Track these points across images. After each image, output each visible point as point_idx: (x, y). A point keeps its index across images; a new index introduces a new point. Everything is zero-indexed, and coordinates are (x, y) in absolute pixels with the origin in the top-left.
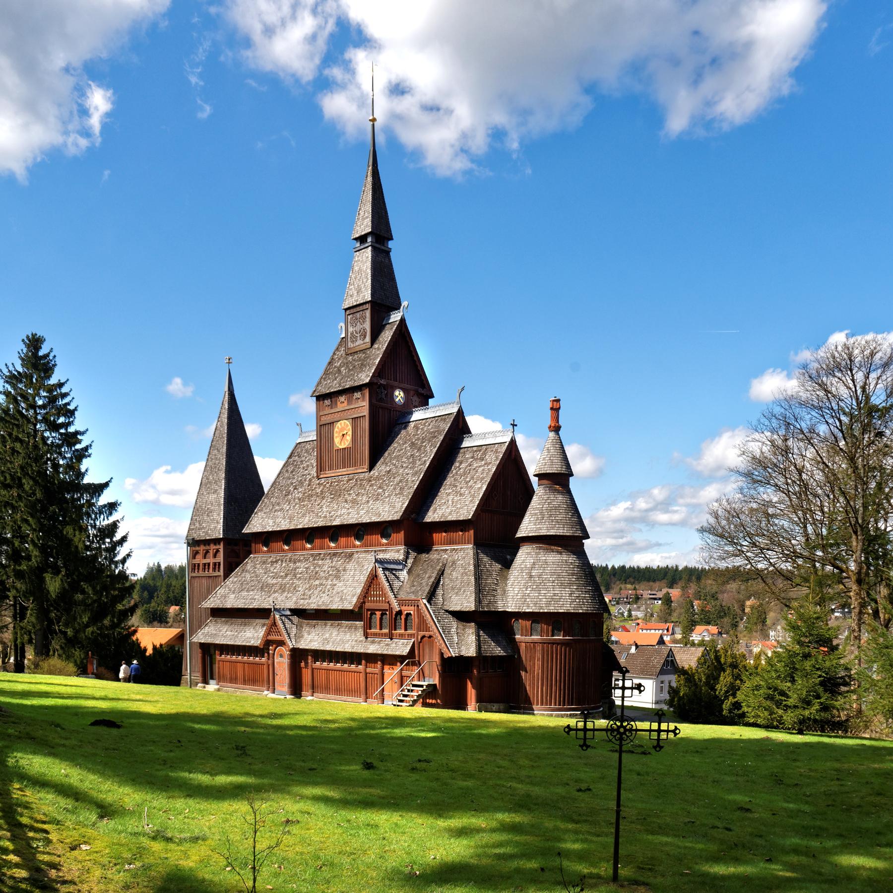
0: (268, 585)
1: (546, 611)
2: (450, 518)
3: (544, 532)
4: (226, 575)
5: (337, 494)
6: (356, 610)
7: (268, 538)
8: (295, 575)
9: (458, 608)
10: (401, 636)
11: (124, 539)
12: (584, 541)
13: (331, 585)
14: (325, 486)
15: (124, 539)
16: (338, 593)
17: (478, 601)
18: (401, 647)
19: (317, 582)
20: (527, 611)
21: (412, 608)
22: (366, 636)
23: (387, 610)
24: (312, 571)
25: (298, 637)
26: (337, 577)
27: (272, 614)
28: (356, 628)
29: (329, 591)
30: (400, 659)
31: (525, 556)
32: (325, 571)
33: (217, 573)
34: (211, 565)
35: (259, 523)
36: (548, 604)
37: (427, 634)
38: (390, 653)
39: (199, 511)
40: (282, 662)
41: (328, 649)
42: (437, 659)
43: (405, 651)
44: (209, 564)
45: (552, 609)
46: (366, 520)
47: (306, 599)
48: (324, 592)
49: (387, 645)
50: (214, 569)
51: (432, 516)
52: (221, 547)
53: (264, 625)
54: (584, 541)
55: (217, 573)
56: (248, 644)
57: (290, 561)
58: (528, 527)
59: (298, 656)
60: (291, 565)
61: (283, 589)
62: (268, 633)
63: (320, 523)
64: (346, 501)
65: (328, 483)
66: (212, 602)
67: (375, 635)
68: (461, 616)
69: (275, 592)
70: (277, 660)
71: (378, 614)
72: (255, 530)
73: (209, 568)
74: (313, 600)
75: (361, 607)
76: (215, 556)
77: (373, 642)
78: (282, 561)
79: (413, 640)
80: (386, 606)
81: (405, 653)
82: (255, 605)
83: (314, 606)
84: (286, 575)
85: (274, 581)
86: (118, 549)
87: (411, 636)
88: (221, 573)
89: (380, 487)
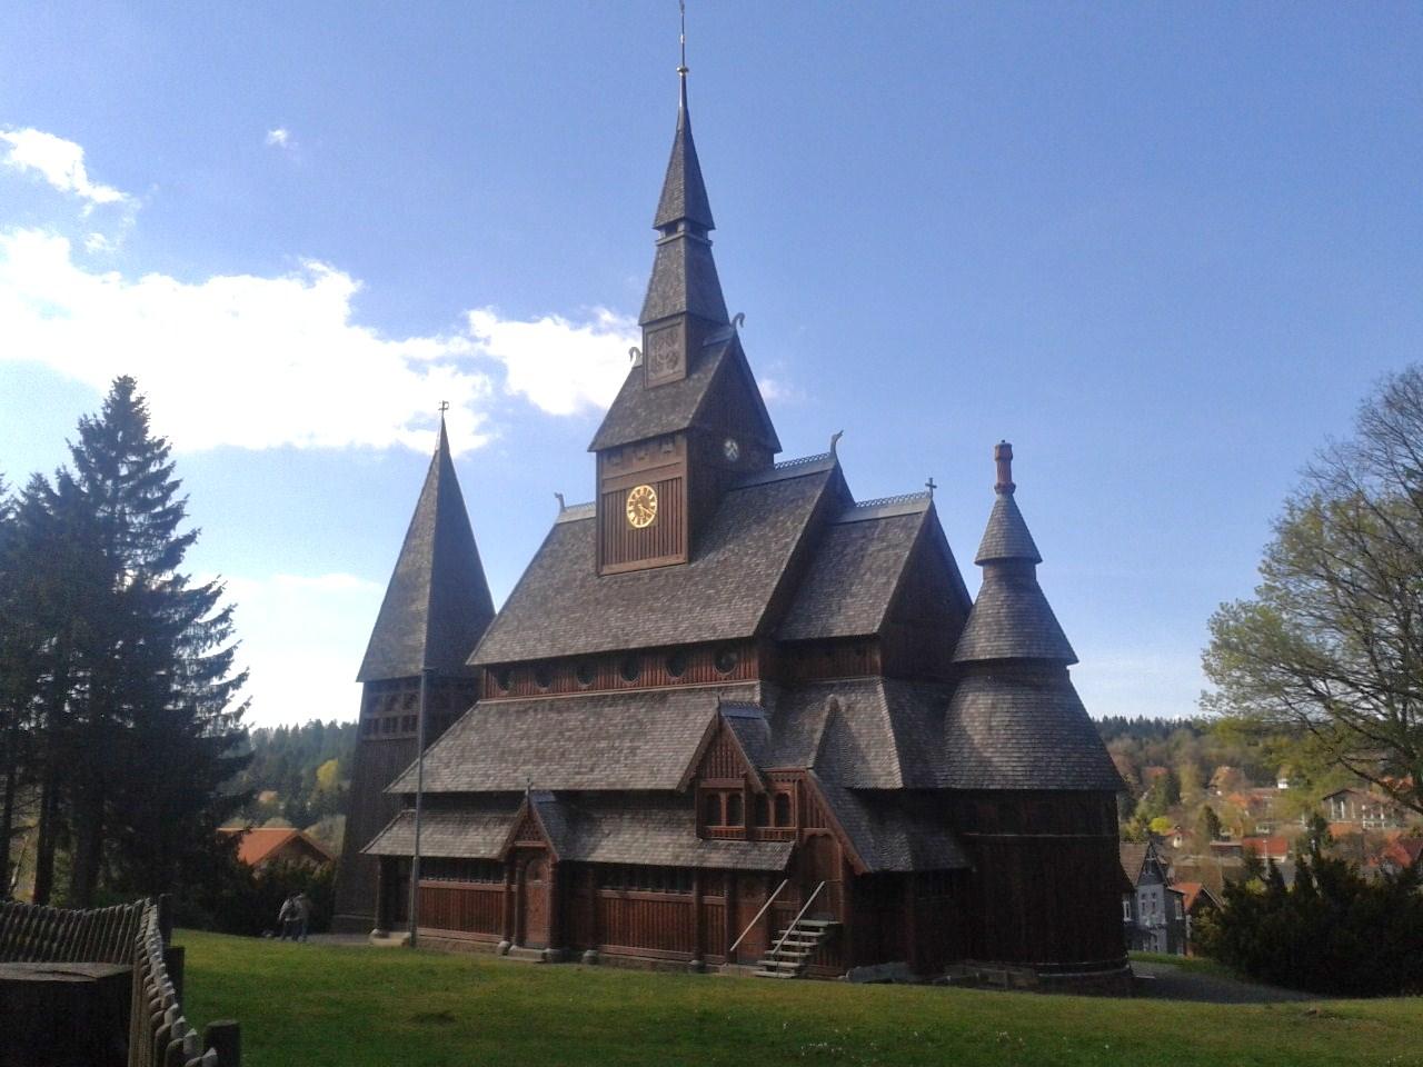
0: (511, 752)
1: (1026, 787)
4: (432, 737)
6: (683, 790)
7: (507, 673)
8: (561, 733)
10: (771, 837)
11: (242, 678)
12: (1069, 667)
13: (629, 748)
14: (610, 587)
15: (242, 678)
16: (646, 761)
18: (773, 855)
19: (603, 744)
20: (991, 787)
21: (791, 785)
22: (704, 835)
23: (741, 789)
24: (594, 726)
27: (526, 800)
28: (679, 824)
29: (626, 759)
30: (772, 878)
32: (616, 725)
33: (410, 734)
34: (400, 720)
35: (494, 649)
38: (749, 866)
40: (541, 887)
41: (628, 861)
43: (781, 863)
44: (395, 719)
45: (1035, 784)
46: (691, 638)
47: (586, 773)
48: (618, 762)
49: (743, 852)
50: (405, 728)
53: (503, 821)
54: (1069, 667)
55: (410, 734)
56: (474, 856)
57: (551, 709)
60: (553, 715)
63: (608, 645)
64: (651, 610)
65: (616, 582)
67: (719, 834)
69: (525, 762)
70: (532, 884)
71: (723, 797)
72: (488, 660)
73: (395, 726)
74: (596, 774)
75: (691, 787)
76: (407, 705)
77: (716, 848)
78: (536, 710)
79: (792, 843)
80: (741, 783)
81: (777, 868)
82: (488, 785)
84: (546, 734)
85: (524, 743)
86: (231, 692)
87: (787, 836)
88: (420, 734)
89: (710, 586)
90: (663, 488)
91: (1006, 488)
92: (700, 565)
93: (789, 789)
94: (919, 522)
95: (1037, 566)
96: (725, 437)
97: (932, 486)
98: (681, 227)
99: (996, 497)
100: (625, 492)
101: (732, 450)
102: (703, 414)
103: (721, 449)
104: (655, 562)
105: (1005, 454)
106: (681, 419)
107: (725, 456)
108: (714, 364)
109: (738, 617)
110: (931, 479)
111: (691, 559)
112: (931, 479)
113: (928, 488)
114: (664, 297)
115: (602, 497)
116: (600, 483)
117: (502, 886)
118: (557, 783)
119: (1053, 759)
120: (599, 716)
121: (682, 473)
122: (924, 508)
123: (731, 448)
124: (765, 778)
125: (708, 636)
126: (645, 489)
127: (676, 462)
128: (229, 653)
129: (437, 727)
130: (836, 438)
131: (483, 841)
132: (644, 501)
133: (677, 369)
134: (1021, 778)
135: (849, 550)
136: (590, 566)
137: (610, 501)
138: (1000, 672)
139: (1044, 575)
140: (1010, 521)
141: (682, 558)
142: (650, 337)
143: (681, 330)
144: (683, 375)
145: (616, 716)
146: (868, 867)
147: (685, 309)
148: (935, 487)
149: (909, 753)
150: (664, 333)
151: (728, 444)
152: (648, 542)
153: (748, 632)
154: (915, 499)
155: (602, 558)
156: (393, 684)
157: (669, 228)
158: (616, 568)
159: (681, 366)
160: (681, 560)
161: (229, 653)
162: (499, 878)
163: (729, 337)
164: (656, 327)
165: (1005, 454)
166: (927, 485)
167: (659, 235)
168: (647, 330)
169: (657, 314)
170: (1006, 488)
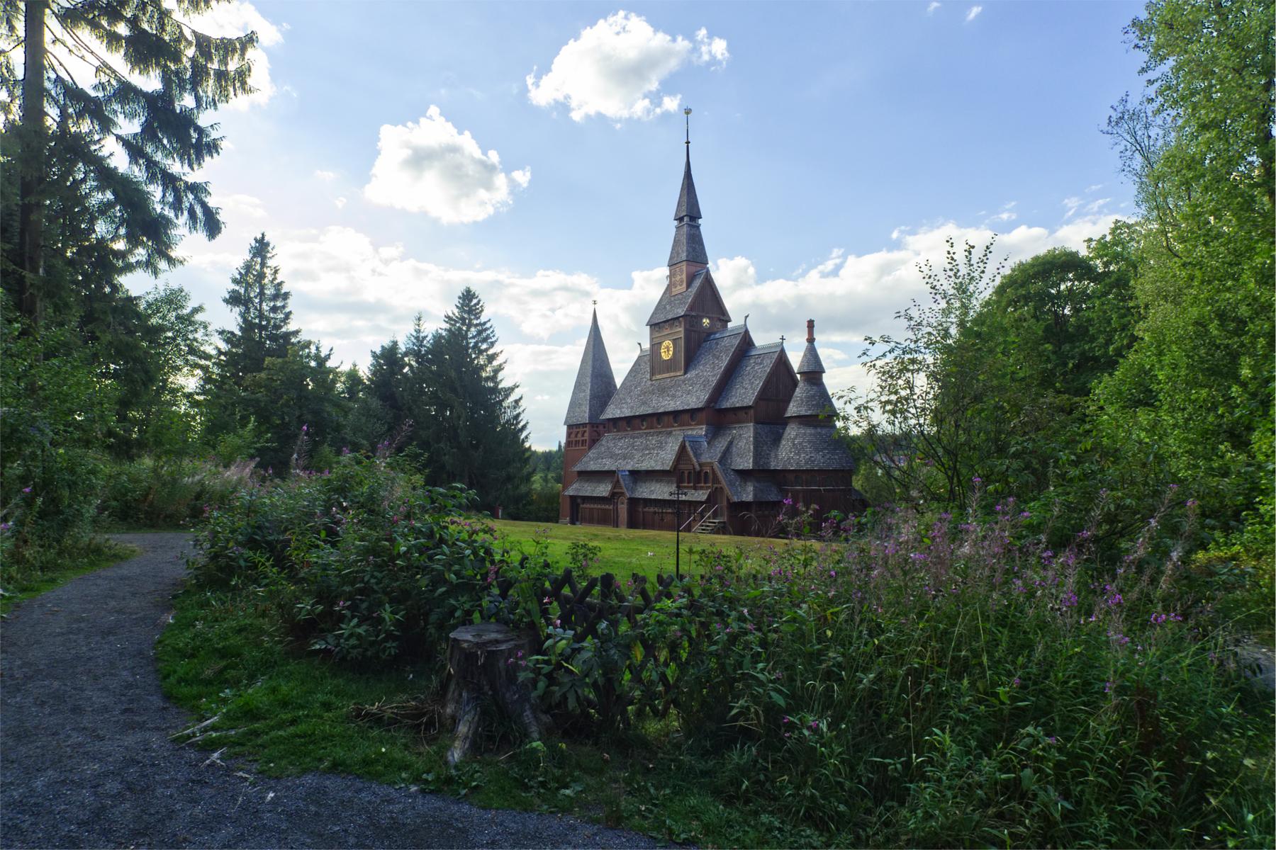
2: (737, 405)
3: (803, 413)
4: (590, 448)
5: (662, 391)
7: (615, 422)
9: (741, 468)
10: (702, 488)
17: (755, 462)
18: (701, 495)
25: (633, 490)
26: (661, 448)
31: (791, 431)
35: (612, 412)
36: (806, 463)
37: (719, 486)
39: (573, 405)
42: (725, 503)
43: (704, 498)
45: (809, 467)
51: (727, 404)
52: (587, 429)
58: (793, 409)
59: (633, 502)
61: (625, 457)
62: (614, 487)
66: (578, 467)
67: (685, 487)
68: (744, 474)
70: (620, 506)
74: (644, 464)
82: (606, 468)
83: (644, 468)
90: (674, 341)
91: (811, 340)
92: (688, 375)
93: (708, 469)
94: (776, 355)
96: (702, 317)
98: (686, 219)
99: (806, 344)
100: (660, 344)
102: (691, 308)
103: (701, 323)
104: (672, 374)
105: (811, 325)
108: (697, 283)
109: (695, 397)
111: (685, 373)
115: (652, 346)
116: (652, 339)
117: (611, 507)
118: (629, 467)
120: (647, 440)
123: (706, 321)
124: (700, 465)
125: (686, 407)
127: (680, 331)
128: (518, 415)
129: (594, 442)
130: (747, 317)
131: (603, 490)
132: (668, 348)
136: (648, 377)
137: (655, 346)
138: (803, 420)
139: (826, 379)
140: (812, 354)
141: (682, 372)
145: (653, 440)
146: (735, 499)
149: (757, 455)
152: (669, 366)
153: (700, 406)
154: (776, 345)
155: (653, 374)
156: (578, 426)
157: (680, 219)
158: (658, 377)
159: (684, 285)
161: (518, 415)
162: (610, 504)
165: (811, 325)
167: (676, 223)
170: (811, 340)
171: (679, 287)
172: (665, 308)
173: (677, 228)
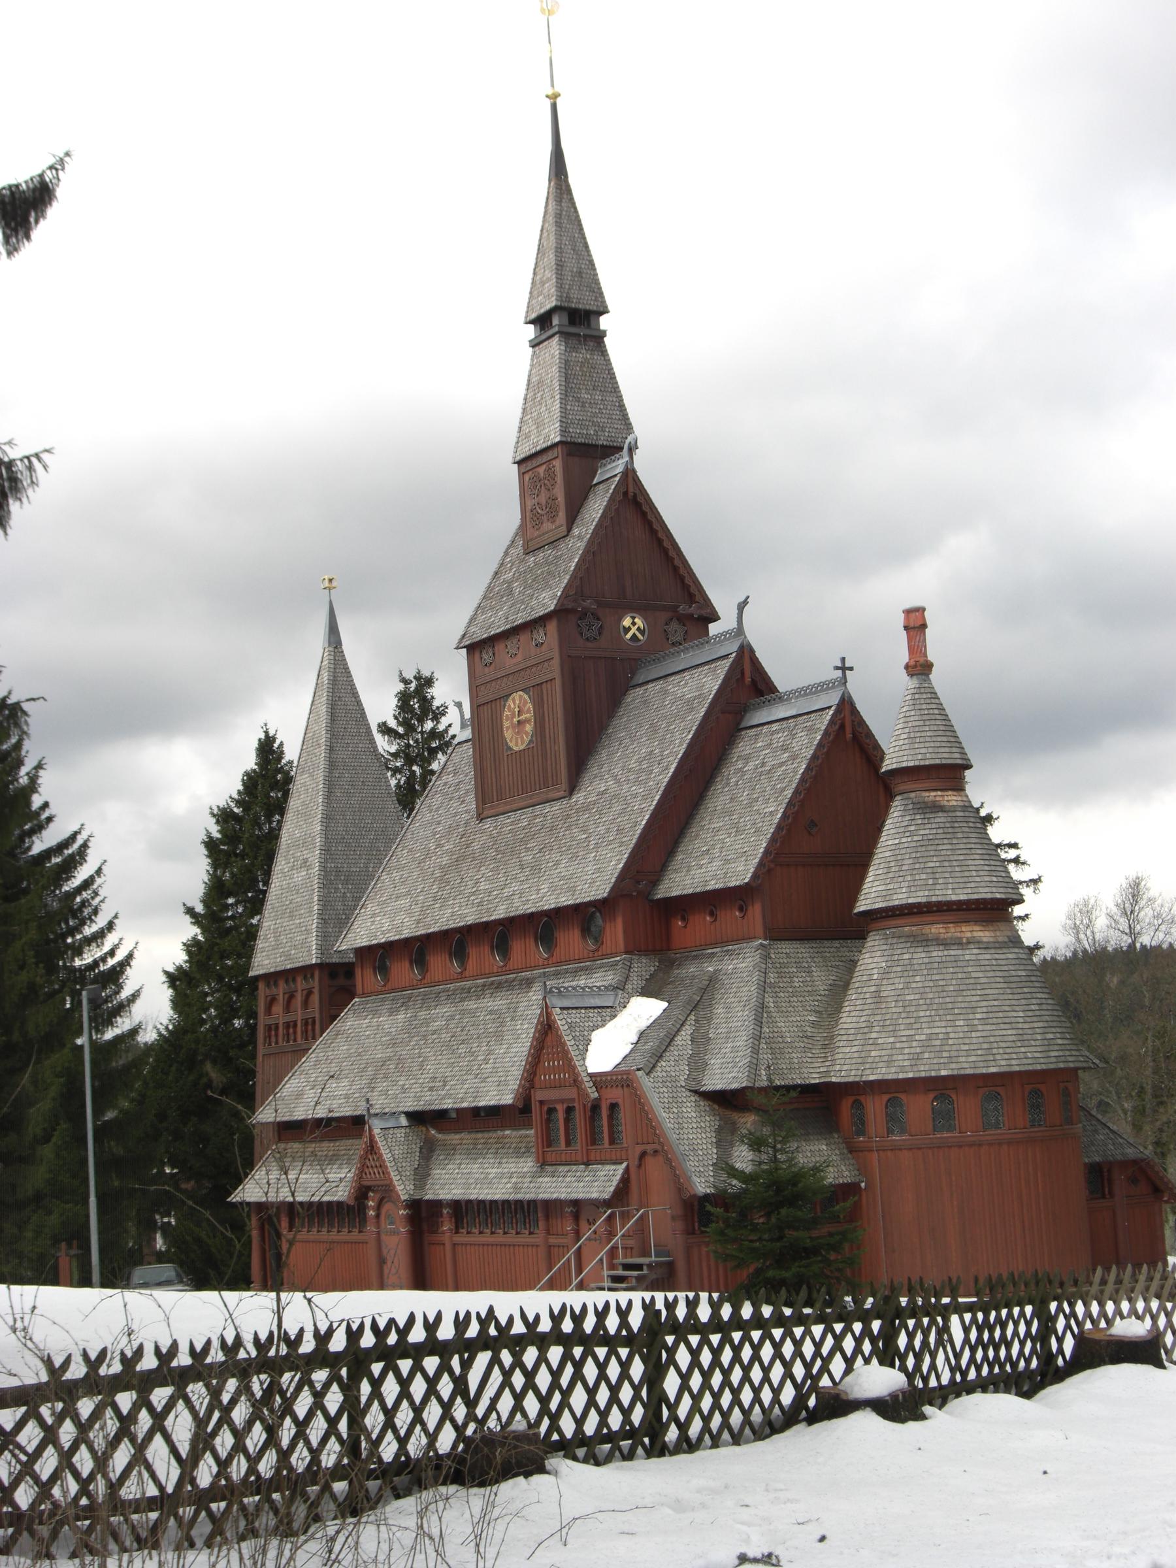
95: (967, 773)
97: (844, 668)
98: (556, 321)
101: (634, 630)
106: (547, 600)
107: (620, 639)
108: (596, 508)
110: (843, 660)
111: (572, 789)
112: (843, 660)
113: (839, 673)
114: (539, 425)
119: (952, 1035)
121: (554, 669)
122: (833, 699)
126: (520, 696)
133: (558, 523)
134: (906, 1063)
135: (751, 766)
141: (564, 785)
142: (527, 477)
143: (558, 465)
144: (564, 528)
147: (558, 439)
148: (851, 669)
150: (541, 470)
151: (627, 622)
160: (562, 793)
163: (620, 469)
164: (530, 465)
166: (837, 668)
167: (530, 331)
168: (524, 468)
169: (527, 450)
171: (547, 526)
172: (510, 592)
173: (535, 344)
